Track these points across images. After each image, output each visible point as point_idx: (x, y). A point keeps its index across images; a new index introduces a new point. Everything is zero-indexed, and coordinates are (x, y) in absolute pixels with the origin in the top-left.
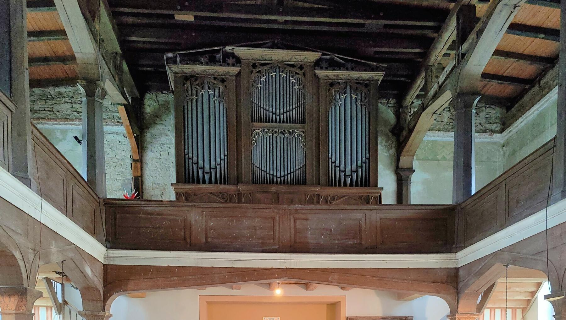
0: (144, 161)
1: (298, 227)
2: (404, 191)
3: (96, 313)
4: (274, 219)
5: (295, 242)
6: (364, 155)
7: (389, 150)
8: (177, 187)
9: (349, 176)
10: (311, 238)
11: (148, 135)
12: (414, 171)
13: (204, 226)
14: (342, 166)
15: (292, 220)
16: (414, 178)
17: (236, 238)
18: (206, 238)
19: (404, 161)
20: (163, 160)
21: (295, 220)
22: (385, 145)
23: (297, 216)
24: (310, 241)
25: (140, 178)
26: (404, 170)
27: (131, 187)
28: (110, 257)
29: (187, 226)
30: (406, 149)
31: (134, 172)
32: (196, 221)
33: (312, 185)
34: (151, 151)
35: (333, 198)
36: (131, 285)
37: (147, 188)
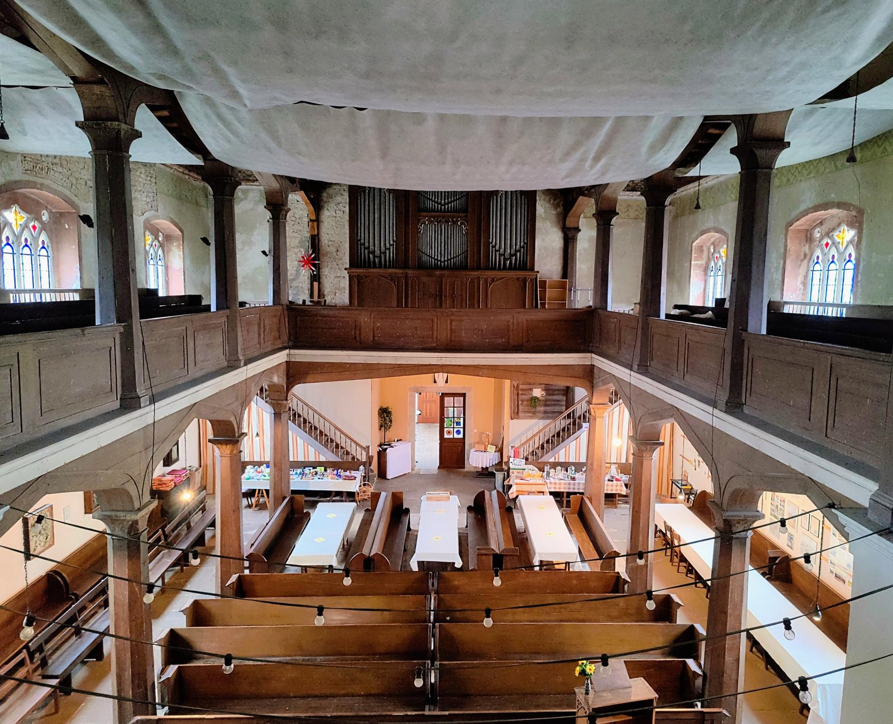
0: (320, 220)
1: (453, 327)
2: (570, 250)
3: (280, 402)
4: (433, 321)
5: (451, 341)
6: (522, 240)
7: (556, 209)
8: (349, 271)
9: (508, 259)
10: (465, 337)
11: (325, 195)
12: (580, 230)
13: (372, 327)
14: (502, 250)
15: (449, 322)
16: (580, 236)
17: (399, 337)
18: (374, 337)
19: (570, 223)
20: (338, 218)
21: (451, 321)
22: (553, 204)
23: (453, 318)
24: (464, 339)
25: (317, 237)
26: (570, 229)
27: (308, 244)
28: (292, 355)
29: (357, 327)
30: (571, 213)
31: (311, 231)
32: (365, 322)
33: (473, 269)
34: (328, 209)
35: (493, 280)
36: (309, 377)
37: (323, 245)
